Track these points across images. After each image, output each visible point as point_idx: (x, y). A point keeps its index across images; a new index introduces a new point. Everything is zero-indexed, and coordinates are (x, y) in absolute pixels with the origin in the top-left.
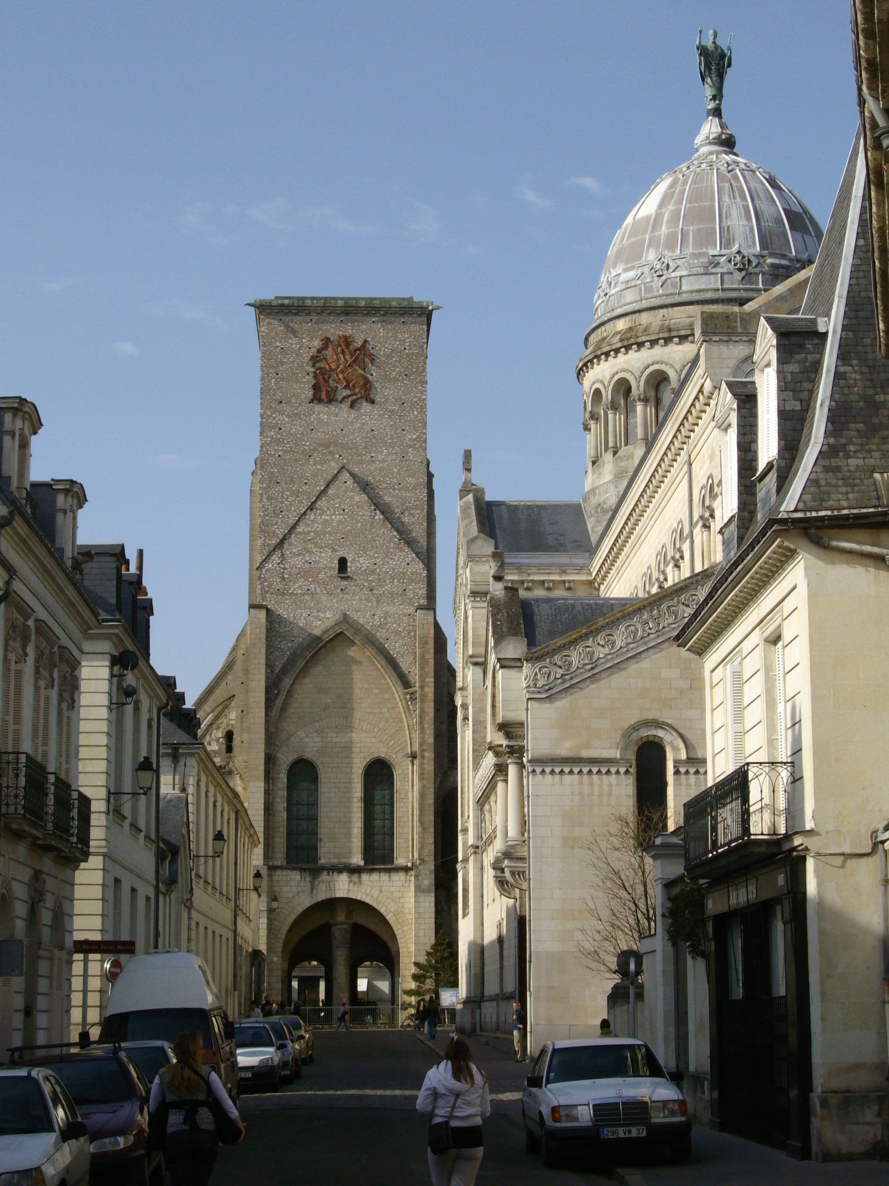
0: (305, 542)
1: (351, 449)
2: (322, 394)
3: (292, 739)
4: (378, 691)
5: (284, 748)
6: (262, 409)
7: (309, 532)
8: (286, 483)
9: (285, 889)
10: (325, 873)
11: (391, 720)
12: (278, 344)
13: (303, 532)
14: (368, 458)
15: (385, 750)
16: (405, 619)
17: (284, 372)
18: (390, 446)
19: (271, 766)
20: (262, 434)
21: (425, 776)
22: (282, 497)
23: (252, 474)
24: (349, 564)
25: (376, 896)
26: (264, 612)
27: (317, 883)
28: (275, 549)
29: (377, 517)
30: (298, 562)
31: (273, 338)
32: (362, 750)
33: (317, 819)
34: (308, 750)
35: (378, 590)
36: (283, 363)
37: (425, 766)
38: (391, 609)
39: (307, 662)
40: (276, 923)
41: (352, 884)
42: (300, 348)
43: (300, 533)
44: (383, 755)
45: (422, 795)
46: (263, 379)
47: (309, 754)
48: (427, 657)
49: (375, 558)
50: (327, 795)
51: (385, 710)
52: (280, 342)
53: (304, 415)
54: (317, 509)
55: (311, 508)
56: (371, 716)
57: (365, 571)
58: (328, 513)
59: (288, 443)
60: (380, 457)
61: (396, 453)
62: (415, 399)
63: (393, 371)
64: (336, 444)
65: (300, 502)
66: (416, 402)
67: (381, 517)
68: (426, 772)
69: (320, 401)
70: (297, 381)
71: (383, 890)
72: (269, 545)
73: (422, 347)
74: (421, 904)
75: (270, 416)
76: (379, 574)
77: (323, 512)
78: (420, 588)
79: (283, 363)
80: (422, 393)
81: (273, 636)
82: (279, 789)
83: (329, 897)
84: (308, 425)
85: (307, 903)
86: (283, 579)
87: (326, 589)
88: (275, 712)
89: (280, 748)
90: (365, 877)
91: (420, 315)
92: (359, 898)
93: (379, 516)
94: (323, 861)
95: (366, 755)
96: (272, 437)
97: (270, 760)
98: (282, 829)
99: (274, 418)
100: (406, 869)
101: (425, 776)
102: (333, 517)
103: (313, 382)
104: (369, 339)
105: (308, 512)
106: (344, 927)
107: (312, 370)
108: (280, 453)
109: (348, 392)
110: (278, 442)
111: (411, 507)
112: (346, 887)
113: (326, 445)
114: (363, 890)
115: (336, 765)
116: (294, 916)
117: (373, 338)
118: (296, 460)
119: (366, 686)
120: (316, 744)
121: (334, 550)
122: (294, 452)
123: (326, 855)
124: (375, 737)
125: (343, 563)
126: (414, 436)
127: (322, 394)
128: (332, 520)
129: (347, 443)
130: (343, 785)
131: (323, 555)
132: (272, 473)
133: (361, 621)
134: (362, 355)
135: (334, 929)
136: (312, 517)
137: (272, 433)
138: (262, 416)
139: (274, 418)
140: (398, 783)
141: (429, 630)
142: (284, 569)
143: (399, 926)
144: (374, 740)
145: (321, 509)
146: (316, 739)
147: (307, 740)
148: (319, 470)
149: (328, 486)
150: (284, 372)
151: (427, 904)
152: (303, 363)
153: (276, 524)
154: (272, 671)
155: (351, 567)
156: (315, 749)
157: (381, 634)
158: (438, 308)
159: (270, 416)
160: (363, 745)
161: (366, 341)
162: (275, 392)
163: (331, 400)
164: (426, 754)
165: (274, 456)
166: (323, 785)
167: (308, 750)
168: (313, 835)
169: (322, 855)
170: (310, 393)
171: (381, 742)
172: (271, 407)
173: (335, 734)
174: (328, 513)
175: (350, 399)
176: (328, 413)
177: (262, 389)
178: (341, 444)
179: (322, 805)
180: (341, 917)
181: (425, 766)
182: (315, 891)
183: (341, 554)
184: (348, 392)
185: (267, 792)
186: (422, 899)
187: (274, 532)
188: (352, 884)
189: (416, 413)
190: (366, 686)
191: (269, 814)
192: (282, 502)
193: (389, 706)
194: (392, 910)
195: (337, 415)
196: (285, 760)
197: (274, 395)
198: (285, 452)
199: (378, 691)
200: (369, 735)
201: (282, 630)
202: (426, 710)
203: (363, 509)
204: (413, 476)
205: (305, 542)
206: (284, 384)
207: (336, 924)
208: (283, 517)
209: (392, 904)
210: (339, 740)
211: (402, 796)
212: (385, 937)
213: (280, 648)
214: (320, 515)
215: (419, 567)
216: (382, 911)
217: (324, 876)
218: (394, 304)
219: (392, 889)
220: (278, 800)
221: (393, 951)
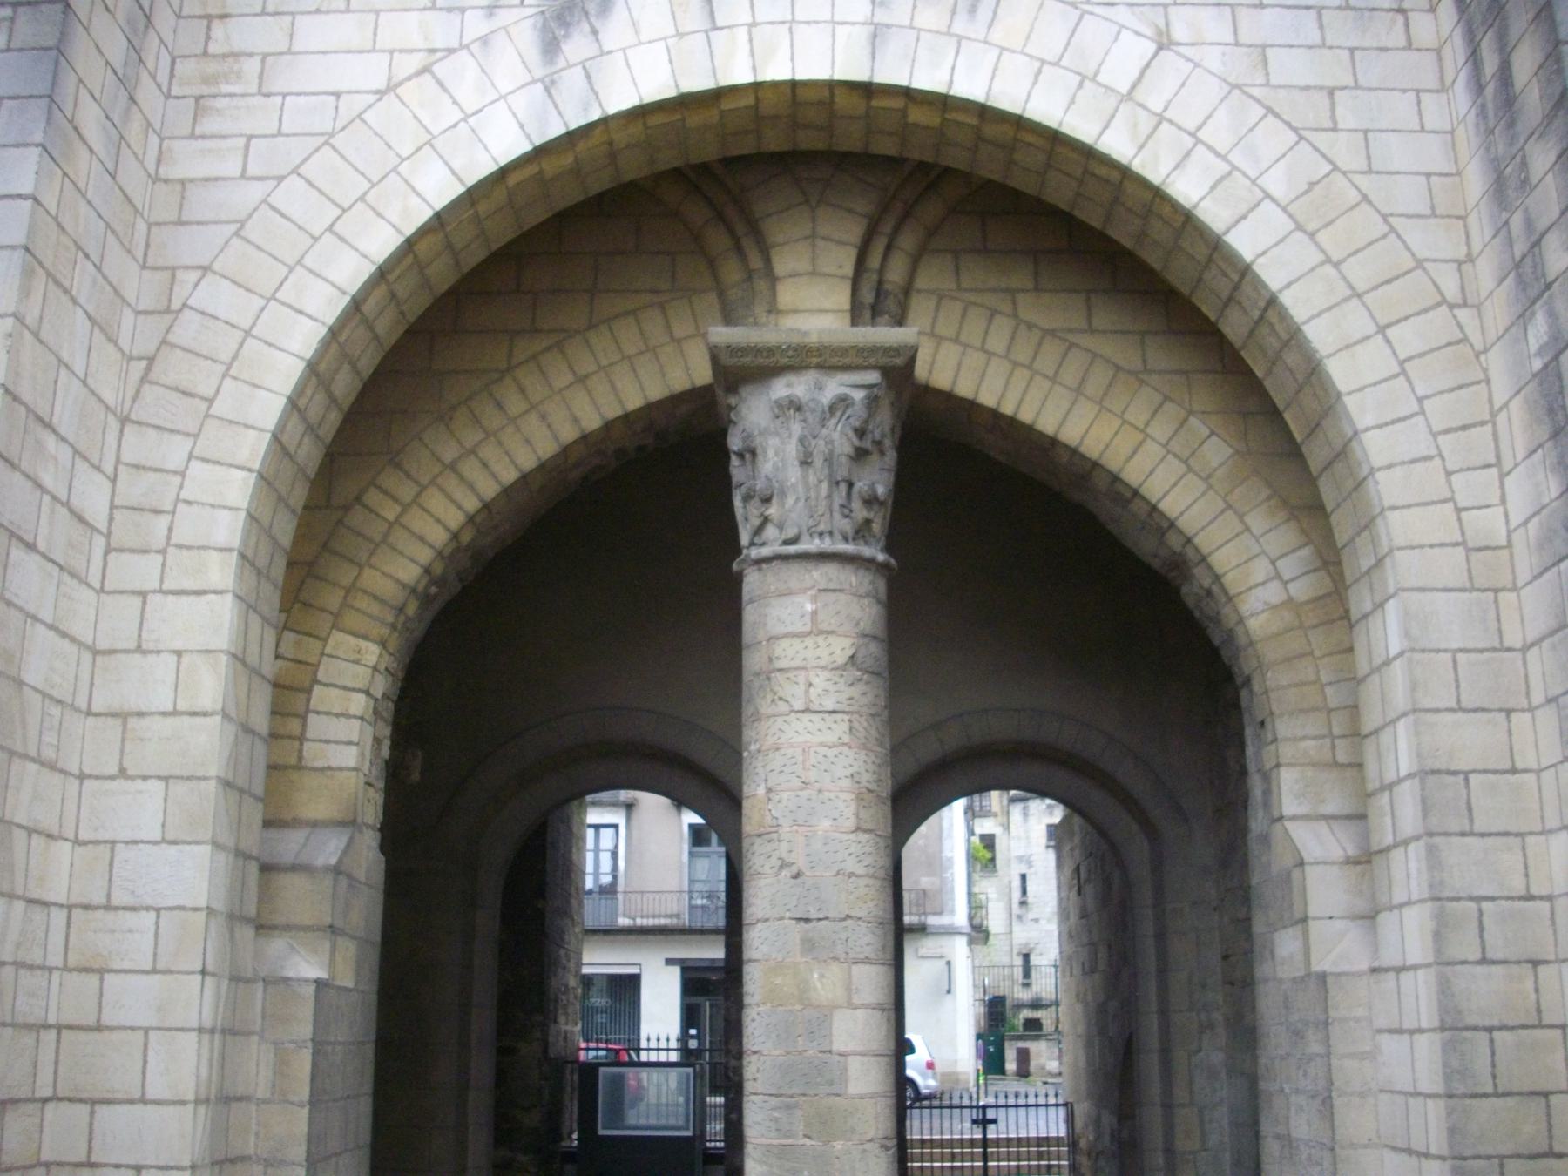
40: (216, 296)
71: (1179, 33)
83: (698, 81)
85: (504, 140)
92: (970, 87)
106: (835, 386)
116: (382, 243)
135: (754, 413)
143: (1356, 321)
180: (810, 301)
182: (576, 47)
194: (1276, 183)
216: (1186, 189)
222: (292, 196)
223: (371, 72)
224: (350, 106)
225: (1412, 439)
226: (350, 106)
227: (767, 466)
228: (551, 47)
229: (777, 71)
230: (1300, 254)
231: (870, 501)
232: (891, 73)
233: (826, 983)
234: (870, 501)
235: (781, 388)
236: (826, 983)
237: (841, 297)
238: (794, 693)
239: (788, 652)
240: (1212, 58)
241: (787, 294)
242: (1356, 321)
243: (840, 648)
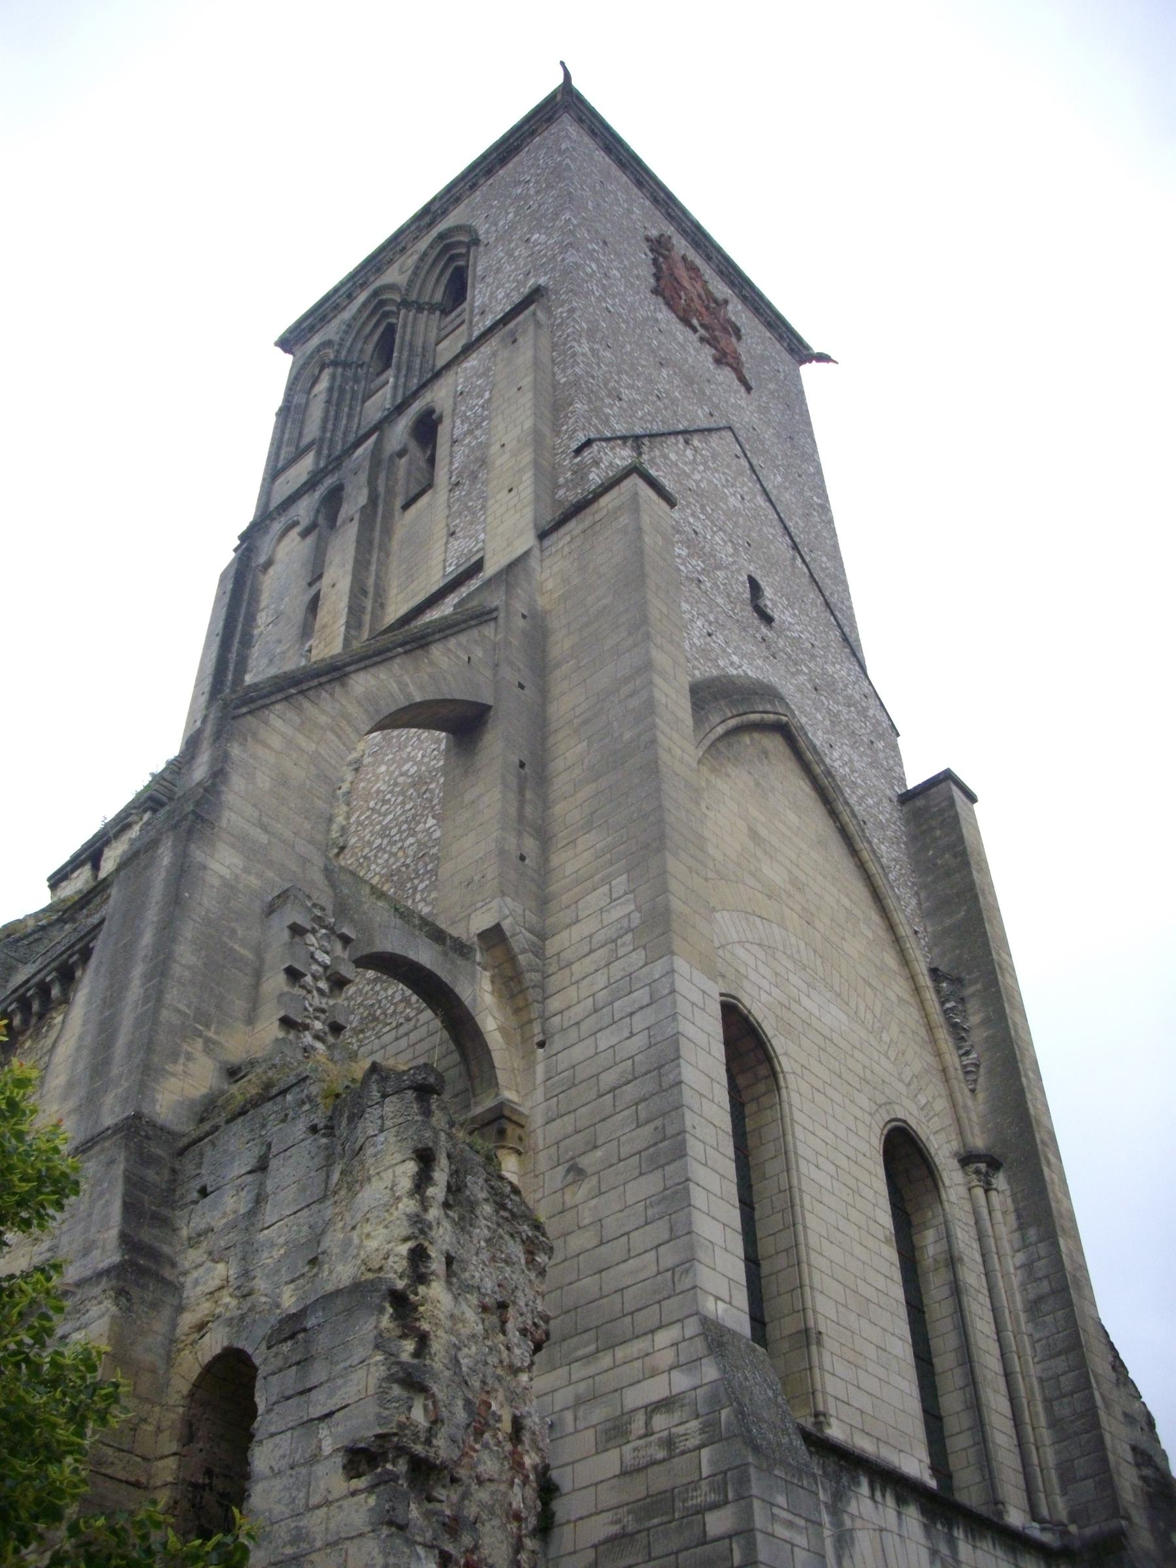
16: (886, 803)
34: (746, 984)
146: (763, 969)
147: (739, 950)
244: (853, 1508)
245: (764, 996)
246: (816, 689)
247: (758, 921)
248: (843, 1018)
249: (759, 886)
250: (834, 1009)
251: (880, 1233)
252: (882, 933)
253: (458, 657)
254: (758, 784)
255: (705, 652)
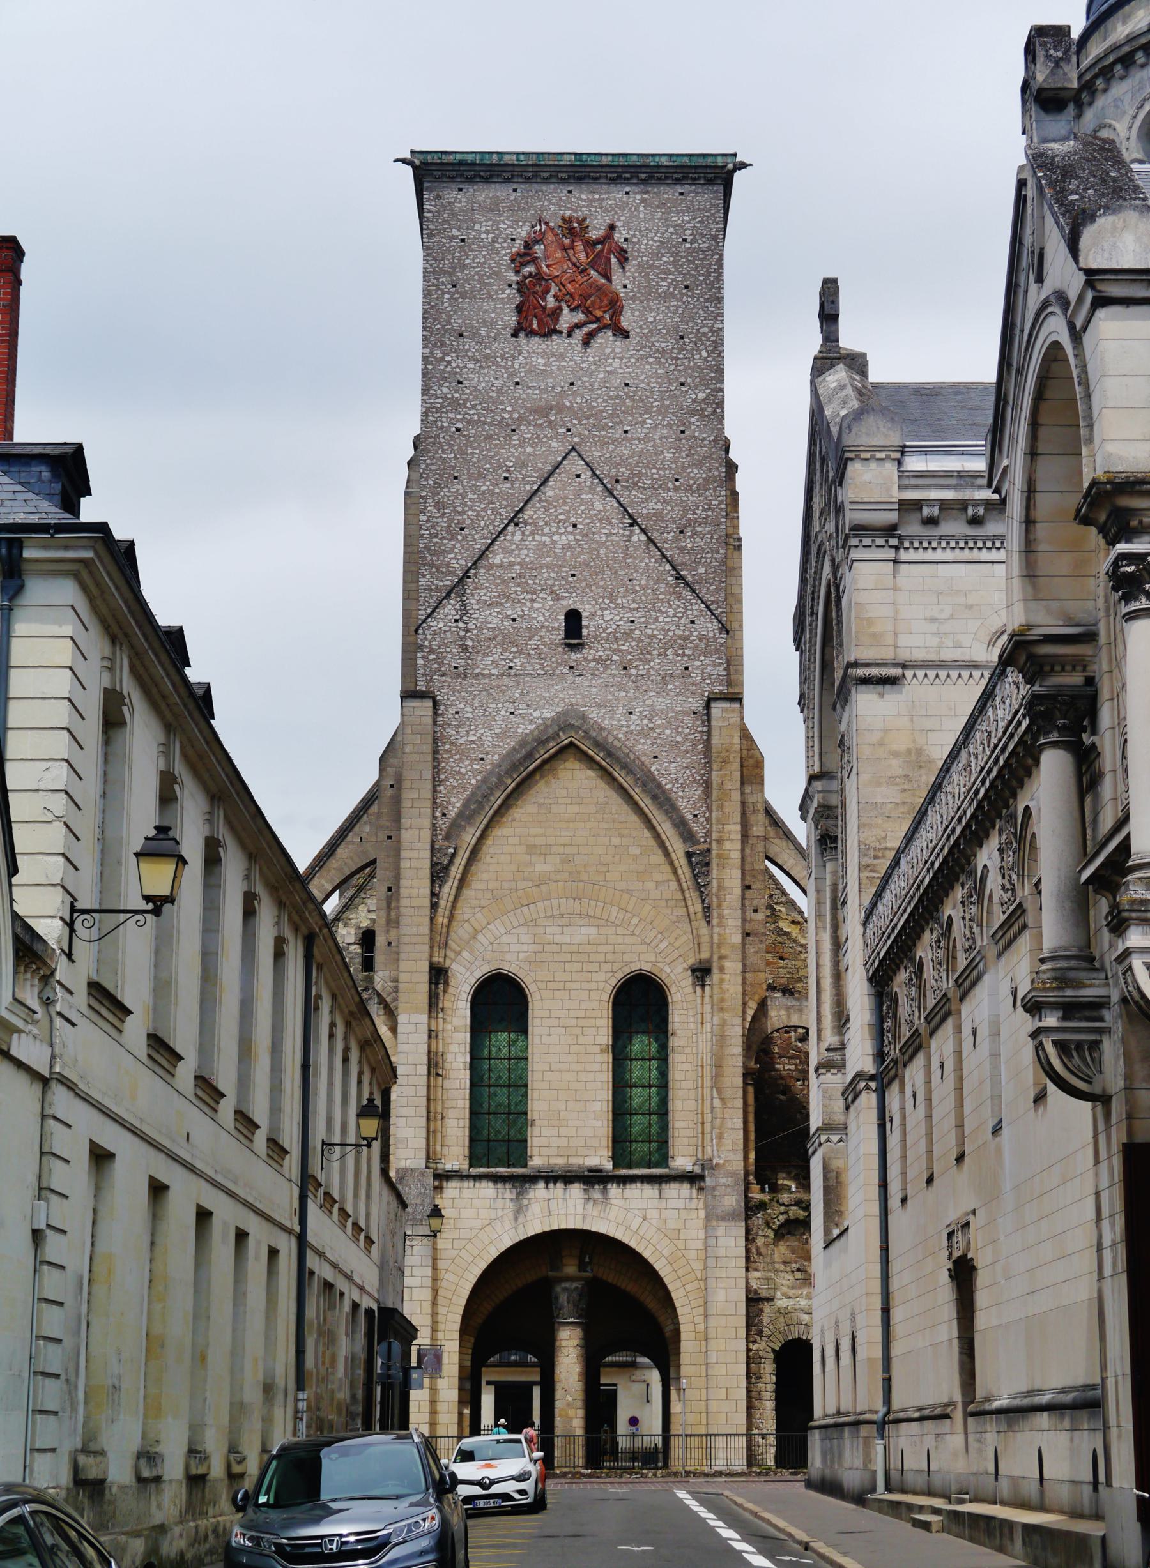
0: (503, 582)
1: (588, 418)
2: (534, 320)
3: (480, 937)
4: (637, 851)
5: (465, 954)
6: (425, 346)
7: (511, 564)
8: (470, 477)
9: (465, 1213)
10: (541, 1184)
11: (663, 904)
12: (455, 232)
13: (501, 565)
14: (618, 434)
15: (653, 959)
16: (688, 721)
17: (466, 281)
18: (659, 412)
19: (441, 987)
20: (425, 392)
21: (725, 1005)
22: (464, 504)
23: (409, 464)
24: (584, 623)
25: (634, 1227)
26: (429, 704)
27: (525, 1202)
28: (448, 595)
29: (635, 538)
30: (493, 619)
31: (445, 221)
32: (610, 957)
33: (526, 1086)
34: (508, 957)
35: (636, 667)
36: (464, 267)
37: (726, 986)
38: (660, 703)
39: (509, 797)
41: (591, 1203)
42: (494, 241)
43: (491, 567)
44: (647, 967)
45: (721, 1039)
46: (427, 293)
47: (511, 966)
48: (728, 785)
49: (631, 610)
50: (545, 1039)
51: (651, 885)
52: (459, 230)
53: (503, 357)
54: (526, 524)
55: (514, 521)
56: (626, 896)
57: (614, 633)
58: (546, 530)
59: (474, 407)
60: (640, 432)
61: (670, 425)
62: (705, 330)
63: (663, 280)
64: (560, 409)
65: (495, 512)
66: (705, 334)
67: (643, 537)
68: (726, 996)
69: (531, 333)
70: (490, 297)
72: (438, 589)
73: (715, 238)
74: (722, 1242)
75: (442, 359)
76: (640, 640)
77: (537, 530)
78: (714, 665)
79: (464, 267)
80: (715, 319)
81: (448, 751)
82: (456, 1030)
84: (511, 375)
85: (507, 1243)
86: (465, 649)
87: (542, 666)
88: (447, 890)
89: (459, 954)
90: (614, 1190)
91: (710, 182)
93: (638, 537)
94: (537, 1161)
95: (616, 967)
96: (445, 398)
97: (438, 975)
98: (461, 1104)
99: (449, 363)
100: (692, 1179)
101: (725, 1005)
102: (556, 538)
103: (518, 299)
104: (618, 224)
105: (510, 528)
106: (575, 1285)
107: (513, 277)
108: (459, 425)
109: (580, 317)
110: (456, 405)
111: (696, 521)
112: (580, 1209)
113: (542, 411)
114: (612, 1216)
115: (561, 985)
117: (626, 225)
118: (489, 437)
119: (616, 841)
120: (525, 948)
121: (558, 598)
122: (484, 423)
123: (543, 1152)
124: (633, 934)
125: (573, 620)
126: (701, 395)
127: (534, 320)
128: (554, 542)
129: (580, 409)
130: (573, 1022)
131: (536, 605)
132: (444, 461)
133: (606, 723)
134: (606, 251)
135: (558, 1289)
136: (518, 538)
137: (445, 390)
138: (425, 359)
139: (449, 363)
140: (677, 1018)
141: (732, 737)
142: (467, 630)
143: (679, 1284)
144: (630, 940)
145: (534, 524)
146: (524, 939)
147: (505, 939)
148: (529, 455)
149: (545, 482)
150: (466, 281)
151: (731, 1242)
152: (499, 265)
153: (452, 551)
154: (444, 815)
155: (589, 627)
156: (522, 956)
157: (642, 748)
158: (743, 166)
159: (442, 359)
160: (610, 948)
161: (612, 227)
162: (450, 317)
163: (549, 332)
164: (727, 964)
165: (448, 429)
166: (537, 1022)
167: (508, 957)
168: (519, 1116)
169: (535, 1152)
170: (513, 320)
171: (643, 942)
172: (443, 344)
173: (558, 930)
174: (546, 530)
175: (586, 329)
176: (545, 355)
177: (425, 312)
178: (571, 408)
179: (536, 1058)
181: (726, 986)
182: (521, 1220)
183: (569, 603)
184: (580, 317)
185: (432, 1034)
186: (721, 1231)
187: (448, 565)
188: (591, 1203)
189: (704, 354)
190: (616, 841)
191: (438, 1075)
192: (463, 513)
193: (657, 877)
194: (665, 1253)
195: (561, 357)
196: (464, 980)
197: (449, 323)
198: (469, 422)
199: (637, 851)
200: (620, 930)
201: (461, 741)
202: (727, 884)
203: (611, 523)
204: (700, 465)
205: (503, 582)
206: (465, 303)
207: (561, 1280)
208: (465, 538)
209: (666, 1241)
210: (567, 939)
211: (682, 1044)
212: (651, 1304)
213: (459, 773)
214: (532, 533)
215: (708, 627)
216: (646, 1255)
217: (540, 1191)
218: (665, 161)
219: (665, 1214)
220: (454, 1048)
221: (668, 1329)
222: (463, 1253)
223: (477, 1224)
224: (475, 1232)
225: (687, 1309)
226: (475, 1232)
227: (561, 1300)
228: (516, 1219)
229: (563, 1227)
230: (668, 1268)
231: (582, 1309)
232: (587, 1227)
233: (571, 1413)
234: (582, 1309)
235: (564, 1285)
236: (571, 1413)
237: (576, 1262)
238: (565, 1351)
239: (564, 1343)
240: (654, 1222)
241: (565, 1261)
242: (679, 1284)
243: (576, 1342)
244: (531, 1195)
245: (522, 956)
246: (625, 668)
247: (525, 909)
248: (593, 930)
249: (531, 884)
250: (584, 930)
251: (597, 1049)
252: (652, 842)
253: (353, 843)
254: (541, 805)
255: (504, 735)
